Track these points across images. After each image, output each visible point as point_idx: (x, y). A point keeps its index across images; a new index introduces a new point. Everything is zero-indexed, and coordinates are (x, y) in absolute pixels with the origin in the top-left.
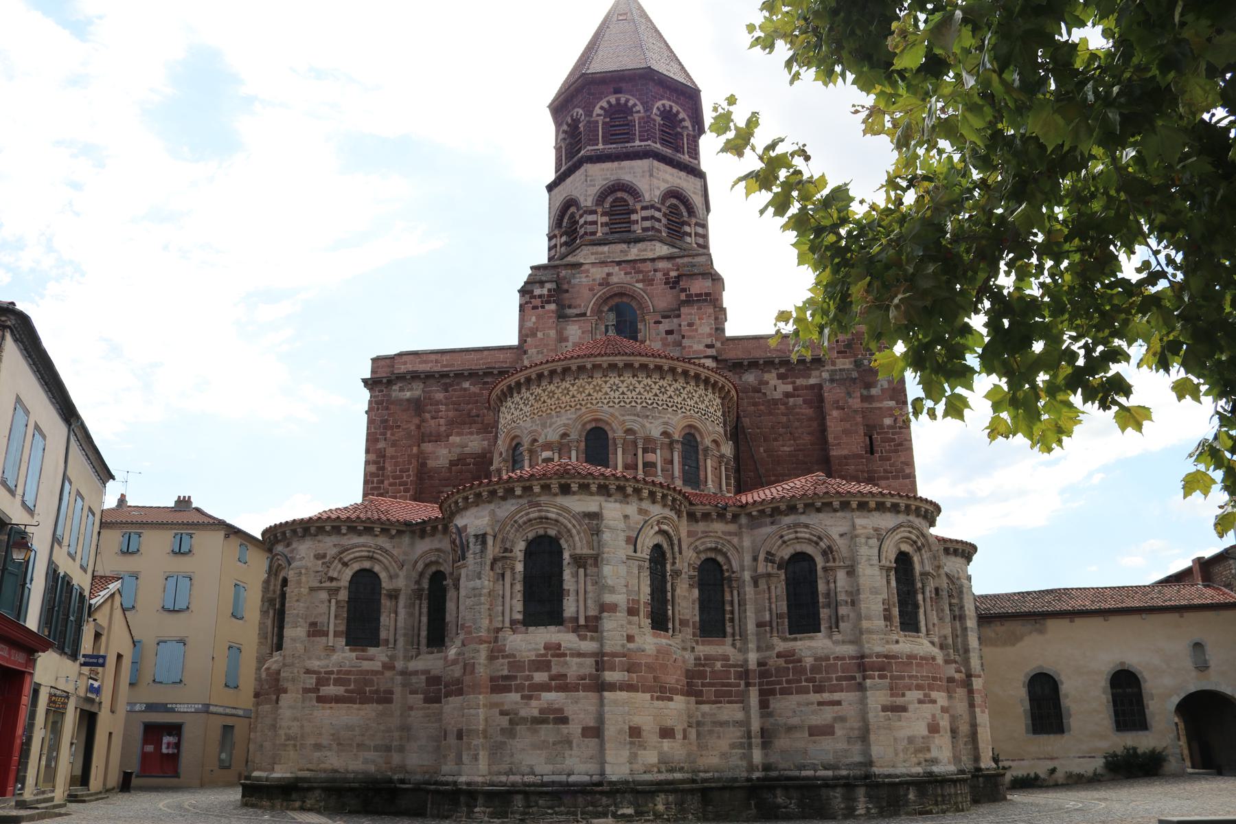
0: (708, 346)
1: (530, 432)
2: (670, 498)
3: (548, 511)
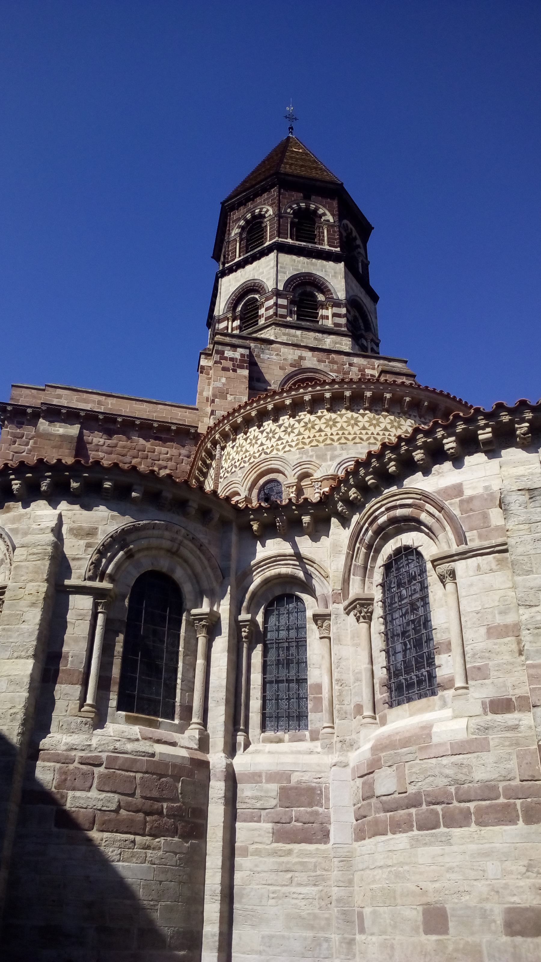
1: (299, 464)
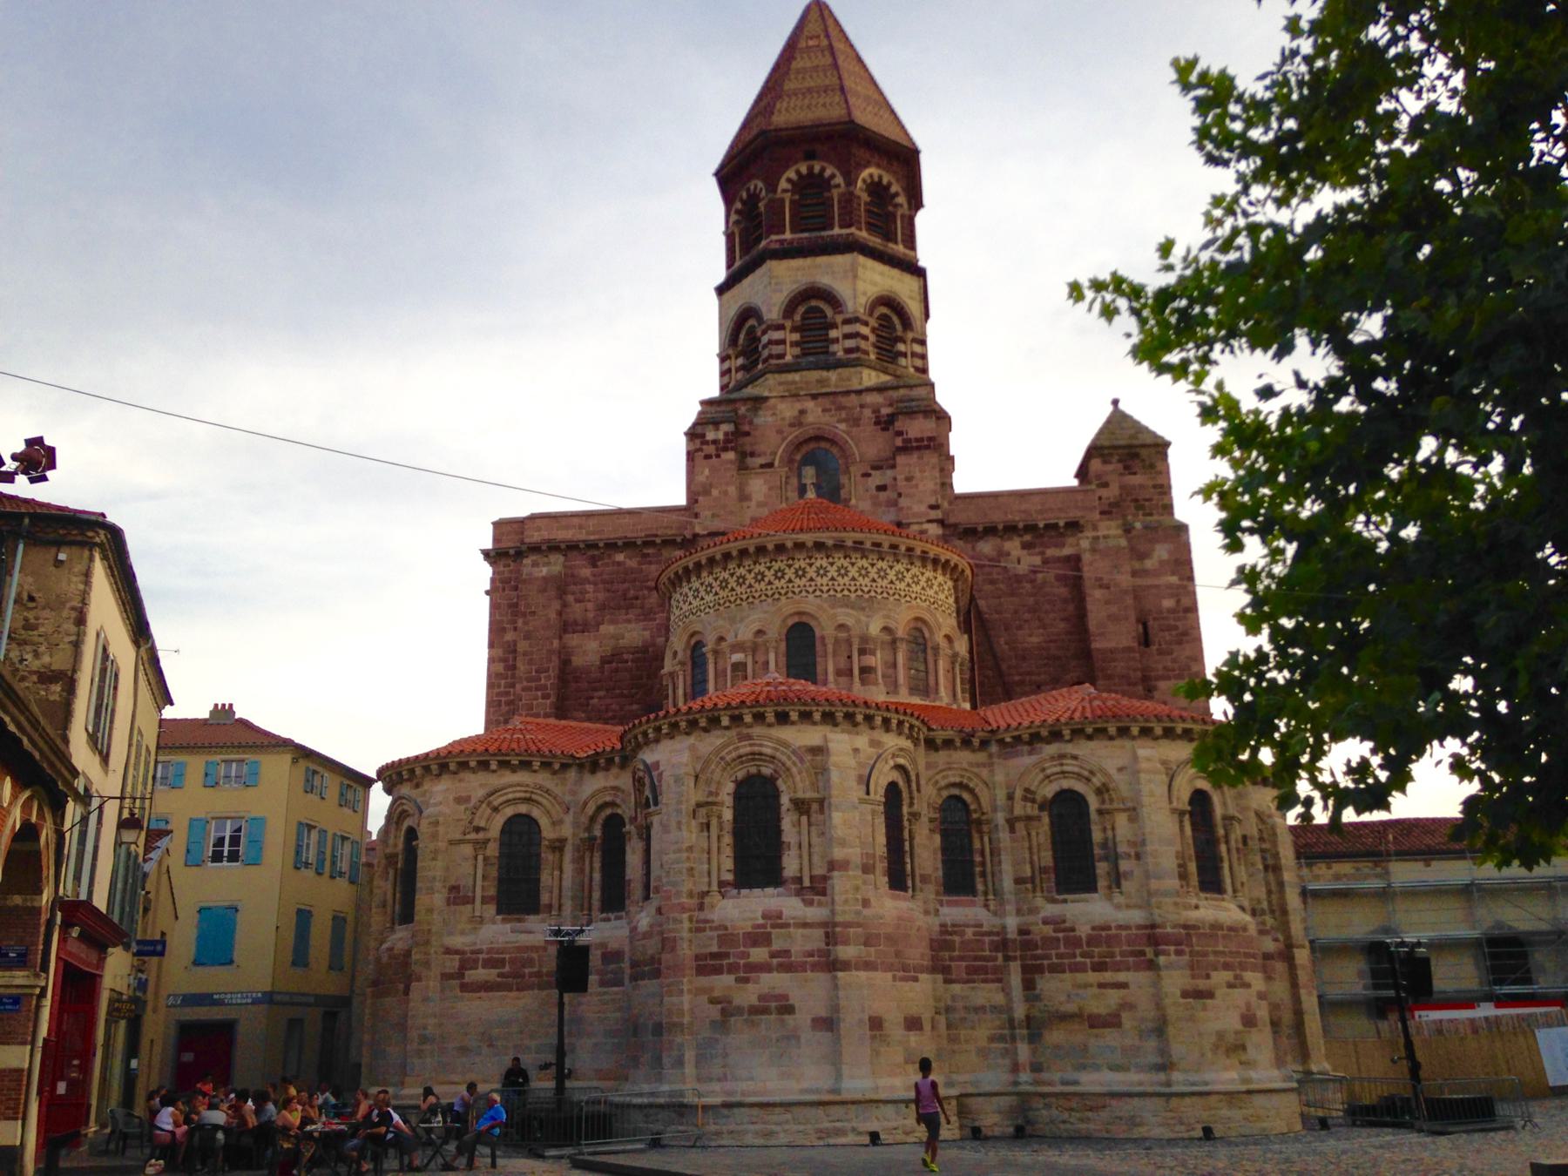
0: (933, 507)
2: (907, 725)
3: (761, 745)
